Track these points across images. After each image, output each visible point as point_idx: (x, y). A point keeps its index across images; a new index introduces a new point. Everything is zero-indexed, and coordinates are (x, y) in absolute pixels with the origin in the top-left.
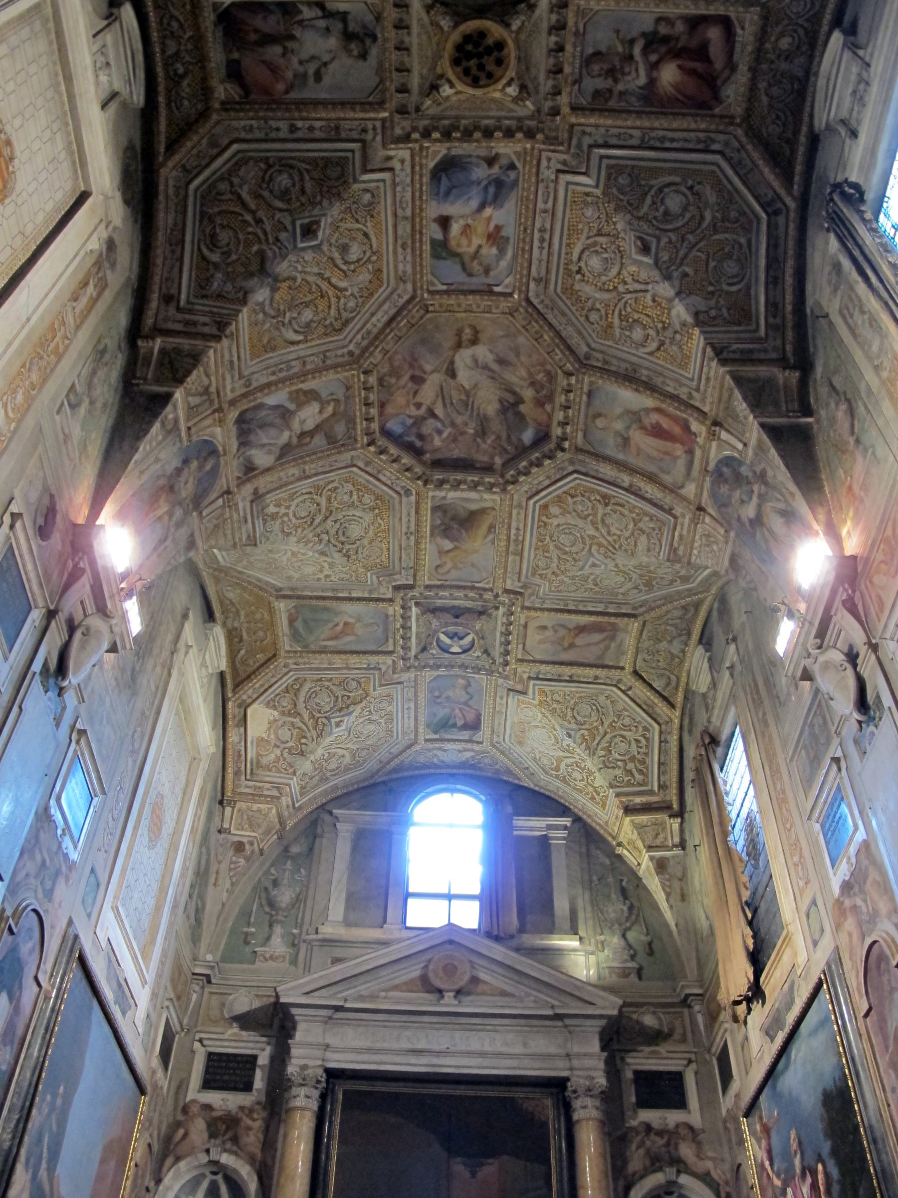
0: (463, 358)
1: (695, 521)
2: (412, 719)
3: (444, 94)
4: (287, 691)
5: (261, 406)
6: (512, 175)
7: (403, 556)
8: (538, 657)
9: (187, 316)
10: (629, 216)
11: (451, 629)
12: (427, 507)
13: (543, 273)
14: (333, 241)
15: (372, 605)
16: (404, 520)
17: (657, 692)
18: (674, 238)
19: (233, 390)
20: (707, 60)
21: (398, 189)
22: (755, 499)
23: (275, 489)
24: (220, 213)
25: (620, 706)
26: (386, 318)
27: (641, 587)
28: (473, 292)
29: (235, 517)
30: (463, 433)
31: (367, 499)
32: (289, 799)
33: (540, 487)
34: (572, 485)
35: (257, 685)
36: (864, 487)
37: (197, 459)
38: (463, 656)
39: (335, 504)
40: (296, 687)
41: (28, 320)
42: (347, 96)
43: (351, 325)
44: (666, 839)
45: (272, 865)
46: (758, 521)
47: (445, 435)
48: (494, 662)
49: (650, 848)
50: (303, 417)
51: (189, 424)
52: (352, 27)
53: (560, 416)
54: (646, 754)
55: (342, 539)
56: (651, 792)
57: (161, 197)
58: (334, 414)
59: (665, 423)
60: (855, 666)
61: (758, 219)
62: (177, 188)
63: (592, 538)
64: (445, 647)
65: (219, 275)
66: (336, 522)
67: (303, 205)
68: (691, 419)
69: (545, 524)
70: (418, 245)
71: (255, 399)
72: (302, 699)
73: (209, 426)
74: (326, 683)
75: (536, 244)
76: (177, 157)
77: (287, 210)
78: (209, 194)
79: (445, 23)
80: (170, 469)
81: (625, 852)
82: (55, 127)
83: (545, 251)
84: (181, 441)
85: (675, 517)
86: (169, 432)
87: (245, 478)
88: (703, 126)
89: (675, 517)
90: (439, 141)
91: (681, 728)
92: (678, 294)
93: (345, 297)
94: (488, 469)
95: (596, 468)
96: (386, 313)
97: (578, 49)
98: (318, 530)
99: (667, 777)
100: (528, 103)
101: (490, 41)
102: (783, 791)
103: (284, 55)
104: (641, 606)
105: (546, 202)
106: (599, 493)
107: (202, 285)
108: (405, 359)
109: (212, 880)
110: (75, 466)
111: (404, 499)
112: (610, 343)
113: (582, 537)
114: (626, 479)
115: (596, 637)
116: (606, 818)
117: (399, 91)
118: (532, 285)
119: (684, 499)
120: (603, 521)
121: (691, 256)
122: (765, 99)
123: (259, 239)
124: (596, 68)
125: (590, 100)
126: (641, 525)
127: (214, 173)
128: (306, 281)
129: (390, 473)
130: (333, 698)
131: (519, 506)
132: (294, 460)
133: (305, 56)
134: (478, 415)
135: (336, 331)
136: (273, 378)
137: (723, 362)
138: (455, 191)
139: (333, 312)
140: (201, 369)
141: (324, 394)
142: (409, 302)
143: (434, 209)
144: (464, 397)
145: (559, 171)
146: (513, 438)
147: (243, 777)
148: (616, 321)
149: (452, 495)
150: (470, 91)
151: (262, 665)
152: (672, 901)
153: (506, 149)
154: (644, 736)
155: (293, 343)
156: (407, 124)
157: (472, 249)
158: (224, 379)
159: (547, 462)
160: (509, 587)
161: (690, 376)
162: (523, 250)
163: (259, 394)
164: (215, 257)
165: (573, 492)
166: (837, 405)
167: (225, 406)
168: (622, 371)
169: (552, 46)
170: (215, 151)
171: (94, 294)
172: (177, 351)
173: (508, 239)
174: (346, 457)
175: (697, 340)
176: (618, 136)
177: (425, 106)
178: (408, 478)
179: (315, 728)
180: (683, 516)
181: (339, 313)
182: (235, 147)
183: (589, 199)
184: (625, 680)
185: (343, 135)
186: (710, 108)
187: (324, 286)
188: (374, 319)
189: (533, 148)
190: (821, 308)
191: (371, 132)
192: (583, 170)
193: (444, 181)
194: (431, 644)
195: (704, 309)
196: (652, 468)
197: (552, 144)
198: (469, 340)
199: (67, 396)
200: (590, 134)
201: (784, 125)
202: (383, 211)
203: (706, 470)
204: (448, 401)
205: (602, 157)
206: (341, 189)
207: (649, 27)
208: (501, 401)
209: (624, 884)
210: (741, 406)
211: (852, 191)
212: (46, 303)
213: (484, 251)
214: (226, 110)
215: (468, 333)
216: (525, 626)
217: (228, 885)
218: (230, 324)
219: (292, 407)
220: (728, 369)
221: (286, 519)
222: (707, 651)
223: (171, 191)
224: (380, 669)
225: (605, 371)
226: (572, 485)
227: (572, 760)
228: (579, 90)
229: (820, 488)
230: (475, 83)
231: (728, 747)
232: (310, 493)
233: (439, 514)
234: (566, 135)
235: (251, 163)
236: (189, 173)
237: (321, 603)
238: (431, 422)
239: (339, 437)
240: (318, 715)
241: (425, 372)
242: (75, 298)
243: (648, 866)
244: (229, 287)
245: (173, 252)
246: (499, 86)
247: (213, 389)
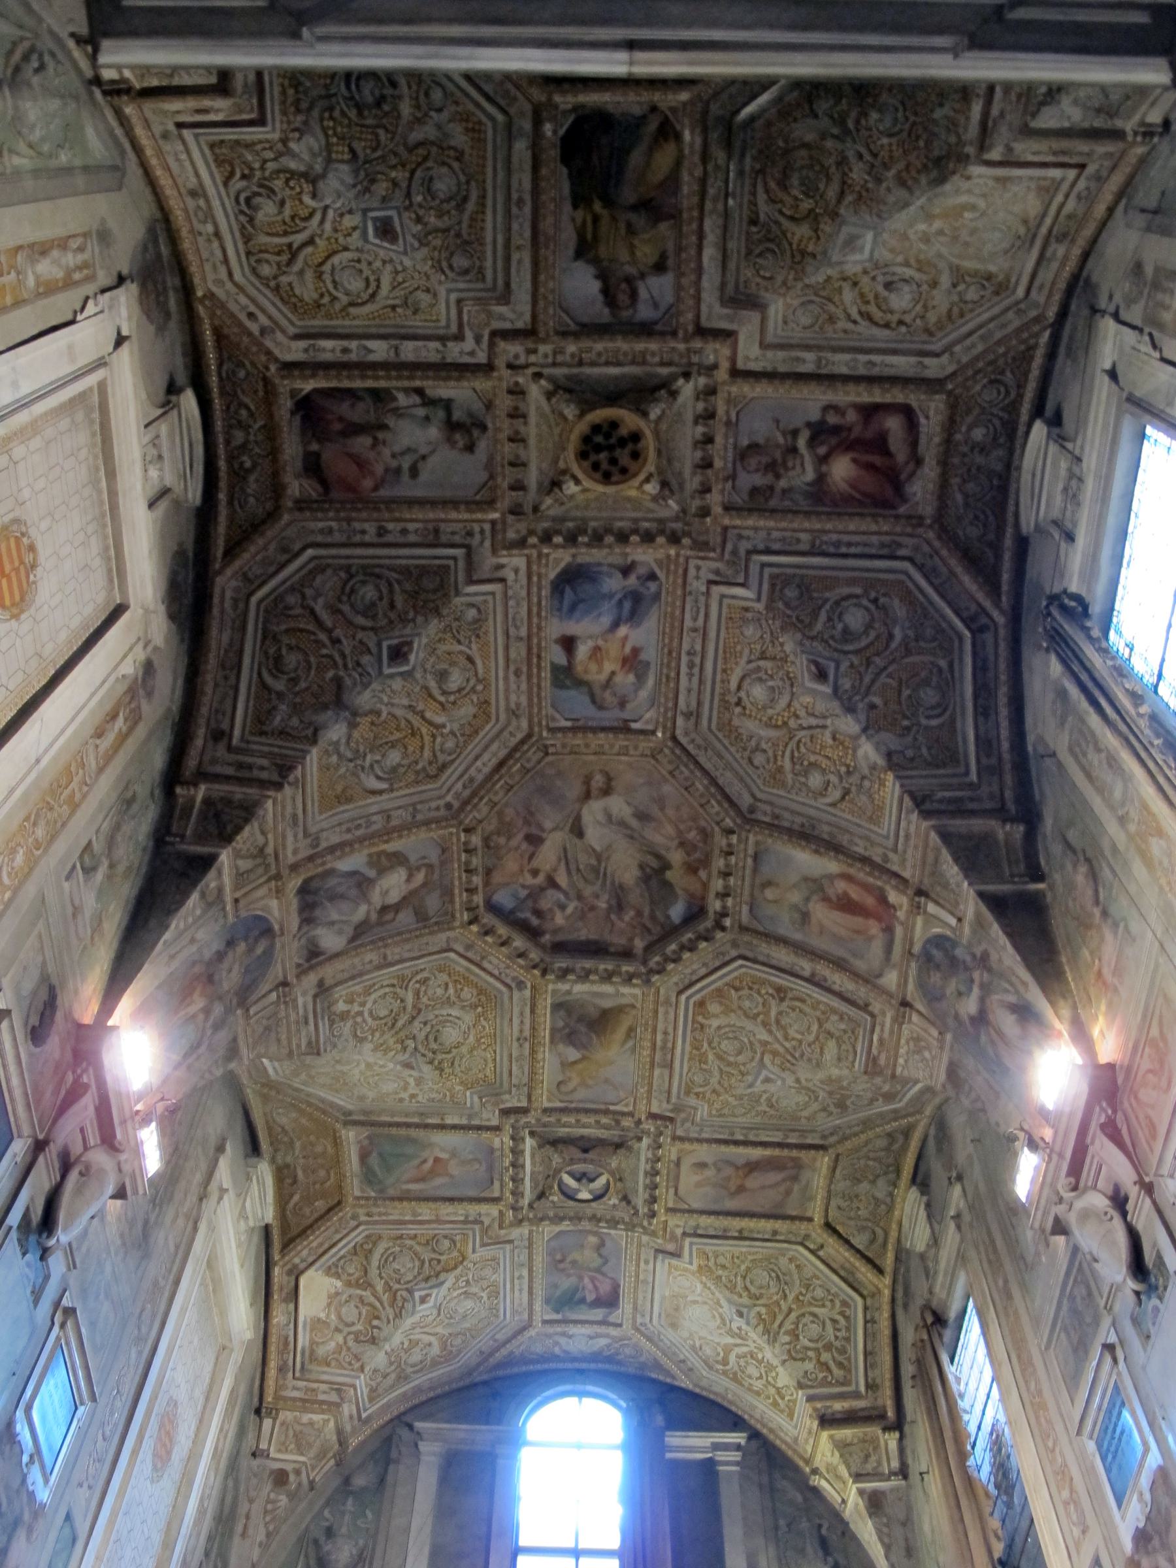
0: (592, 812)
1: (899, 1020)
3: (569, 492)
4: (354, 1252)
5: (331, 872)
6: (653, 586)
7: (514, 1068)
8: (696, 1205)
9: (240, 758)
10: (799, 636)
11: (579, 1168)
12: (546, 1003)
13: (694, 704)
14: (428, 666)
15: (472, 1135)
16: (516, 1021)
17: (858, 1251)
18: (856, 661)
19: (295, 852)
20: (887, 453)
21: (511, 603)
22: (976, 991)
23: (346, 981)
24: (287, 631)
25: (808, 1272)
26: (494, 761)
27: (832, 1108)
28: (603, 729)
29: (293, 1017)
30: (593, 908)
31: (468, 993)
32: (354, 1407)
33: (694, 978)
34: (736, 974)
35: (314, 1244)
36: (1118, 971)
37: (246, 939)
38: (594, 1204)
39: (425, 1000)
40: (366, 1247)
41: (38, 761)
42: (448, 494)
43: (450, 771)
44: (879, 1463)
45: (327, 1503)
46: (981, 1019)
47: (569, 910)
48: (636, 1213)
49: (858, 1477)
50: (385, 887)
51: (238, 895)
52: (457, 415)
53: (718, 884)
54: (847, 1339)
55: (434, 1046)
56: (856, 1395)
57: (216, 611)
59: (855, 893)
60: (1124, 1214)
61: (961, 638)
62: (235, 601)
63: (765, 1044)
64: (569, 1192)
65: (284, 707)
66: (425, 1024)
67: (391, 622)
68: (888, 888)
69: (702, 1026)
70: (535, 671)
71: (324, 864)
73: (262, 898)
74: (409, 1242)
75: (684, 669)
76: (237, 564)
77: (372, 629)
78: (276, 608)
79: (570, 411)
80: (208, 954)
81: (824, 1483)
82: (90, 529)
83: (695, 680)
84: (225, 916)
85: (873, 1016)
86: (210, 905)
87: (306, 965)
88: (885, 528)
89: (873, 1016)
90: (563, 547)
91: (893, 1300)
92: (865, 730)
93: (442, 735)
94: (626, 954)
95: (766, 951)
96: (495, 754)
97: (731, 441)
98: (402, 1034)
99: (877, 1372)
100: (671, 502)
101: (623, 431)
102: (1040, 1392)
103: (374, 446)
104: (832, 1134)
105: (695, 619)
106: (771, 984)
107: (260, 722)
108: (518, 813)
109: (239, 1528)
110: (85, 948)
111: (516, 995)
112: (781, 793)
114: (806, 966)
115: (774, 1177)
116: (795, 1432)
117: (513, 488)
118: (680, 721)
119: (883, 992)
120: (778, 1022)
121: (878, 684)
122: (959, 498)
123: (335, 663)
124: (753, 462)
125: (746, 498)
126: (828, 1026)
127: (284, 582)
128: (394, 716)
129: (497, 959)
130: (417, 1263)
131: (667, 1002)
132: (372, 942)
133: (397, 448)
134: (613, 883)
136: (348, 837)
137: (926, 814)
138: (581, 606)
139: (427, 753)
140: (256, 824)
141: (413, 858)
142: (523, 742)
143: (555, 628)
144: (594, 862)
145: (711, 582)
146: (658, 914)
147: (290, 1374)
148: (787, 764)
149: (579, 988)
150: (601, 488)
151: (321, 1217)
152: (894, 1559)
153: (645, 556)
154: (842, 1313)
155: (374, 792)
156: (523, 527)
157: (603, 677)
158: (284, 837)
159: (703, 945)
160: (655, 1109)
161: (885, 832)
162: (668, 677)
163: (329, 857)
164: (279, 685)
165: (737, 983)
166: (1075, 866)
167: (285, 872)
168: (796, 827)
169: (698, 437)
170: (286, 557)
171: (124, 729)
172: (228, 802)
173: (648, 664)
174: (441, 939)
175: (891, 788)
176: (783, 540)
177: (543, 507)
178: (521, 967)
179: (392, 1305)
180: (884, 1014)
181: (435, 756)
182: (310, 552)
183: (749, 615)
184: (814, 1235)
185: (444, 539)
186: (893, 507)
187: (416, 721)
188: (479, 763)
189: (678, 555)
190: (1046, 745)
191: (478, 537)
192: (741, 580)
193: (569, 594)
194: (551, 1187)
195: (899, 748)
196: (839, 952)
197: (700, 550)
198: (601, 789)
199: (81, 857)
200: (748, 538)
201: (985, 526)
202: (491, 629)
203: (910, 953)
204: (573, 867)
205: (763, 565)
206: (439, 603)
207: (815, 415)
208: (641, 867)
209: (824, 1531)
210: (951, 870)
211: (1073, 604)
212: (62, 740)
213: (618, 679)
214: (300, 509)
215: (598, 781)
216: (678, 1164)
217: (261, 1536)
218: (295, 768)
219: (372, 873)
220: (932, 822)
221: (359, 1019)
222: (922, 1193)
223: (228, 604)
224: (482, 1223)
225: (774, 827)
226: (736, 974)
227: (745, 1349)
228: (733, 487)
229: (1059, 975)
230: (607, 478)
231: (959, 1328)
232: (393, 986)
233: (562, 1013)
234: (719, 540)
235: (329, 572)
236: (251, 583)
237: (403, 1132)
238: (551, 893)
239: (431, 913)
240: (397, 1286)
241: (543, 830)
242: (99, 734)
243: (857, 1505)
244: (295, 721)
245: (226, 678)
246: (636, 482)
247: (270, 850)
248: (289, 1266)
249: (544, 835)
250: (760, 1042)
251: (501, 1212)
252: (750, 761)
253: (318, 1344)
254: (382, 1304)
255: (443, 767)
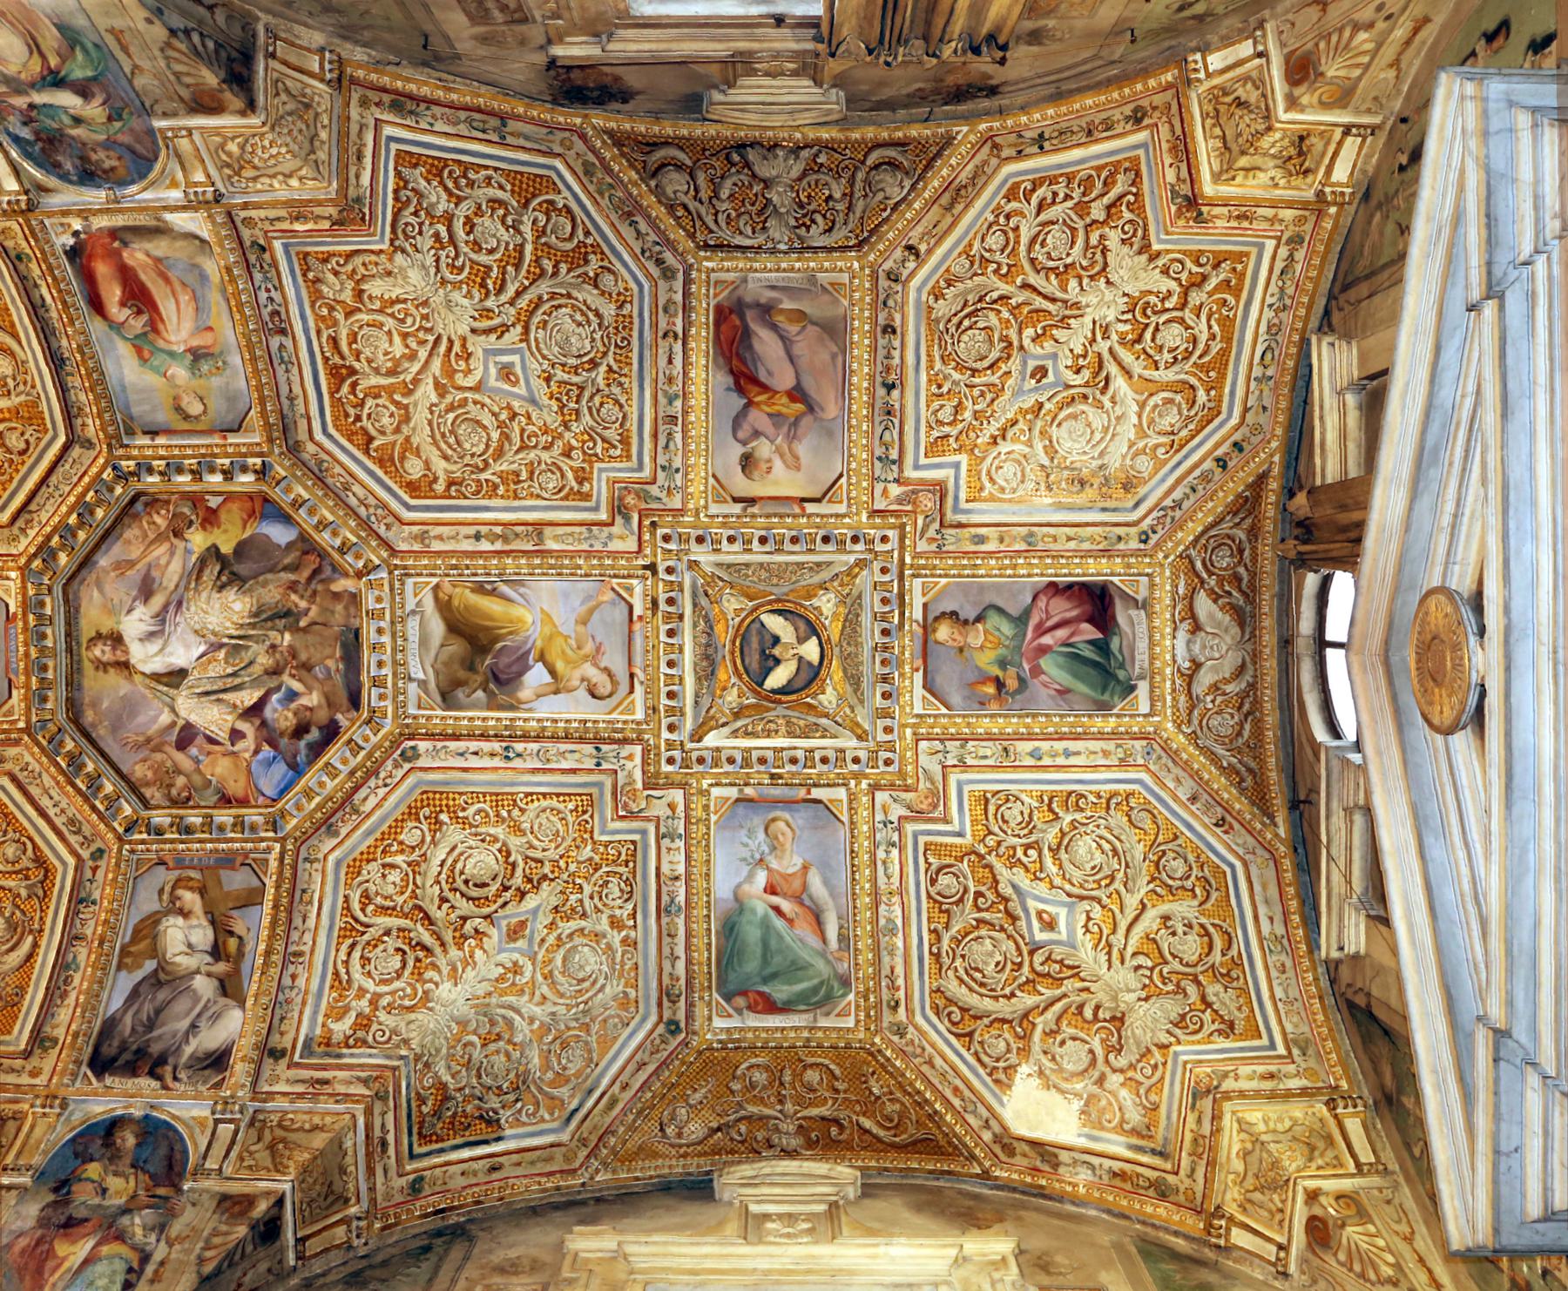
2: (1073, 745)
7: (565, 765)
16: (474, 762)
30: (293, 652)
33: (372, 501)
40: (957, 1017)
47: (296, 686)
55: (494, 888)
58: (202, 891)
63: (441, 390)
64: (804, 677)
66: (443, 900)
69: (451, 483)
72: (988, 1004)
98: (448, 936)
108: (144, 760)
111: (420, 763)
113: (451, 408)
130: (983, 932)
131: (422, 537)
134: (253, 626)
135: (46, 877)
141: (156, 906)
146: (287, 561)
147: (1171, 1179)
155: (30, 956)
160: (632, 545)
188: (51, 812)
198: (114, 648)
204: (230, 682)
208: (221, 588)
219: (150, 965)
221: (385, 1001)
232: (353, 946)
238: (268, 712)
239: (255, 883)
240: (1026, 969)
241: (174, 724)
248: (997, 1150)
249: (181, 723)
250: (442, 396)
251: (875, 787)
252: (23, 453)
253: (1123, 1121)
254: (1059, 999)
255: (40, 861)
